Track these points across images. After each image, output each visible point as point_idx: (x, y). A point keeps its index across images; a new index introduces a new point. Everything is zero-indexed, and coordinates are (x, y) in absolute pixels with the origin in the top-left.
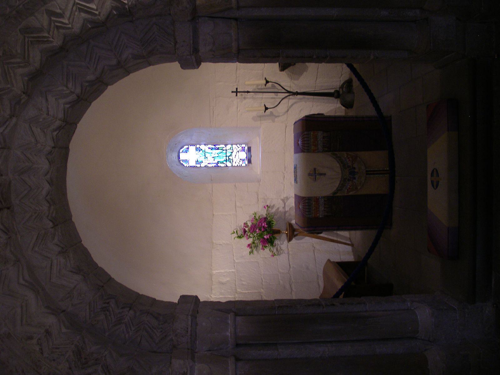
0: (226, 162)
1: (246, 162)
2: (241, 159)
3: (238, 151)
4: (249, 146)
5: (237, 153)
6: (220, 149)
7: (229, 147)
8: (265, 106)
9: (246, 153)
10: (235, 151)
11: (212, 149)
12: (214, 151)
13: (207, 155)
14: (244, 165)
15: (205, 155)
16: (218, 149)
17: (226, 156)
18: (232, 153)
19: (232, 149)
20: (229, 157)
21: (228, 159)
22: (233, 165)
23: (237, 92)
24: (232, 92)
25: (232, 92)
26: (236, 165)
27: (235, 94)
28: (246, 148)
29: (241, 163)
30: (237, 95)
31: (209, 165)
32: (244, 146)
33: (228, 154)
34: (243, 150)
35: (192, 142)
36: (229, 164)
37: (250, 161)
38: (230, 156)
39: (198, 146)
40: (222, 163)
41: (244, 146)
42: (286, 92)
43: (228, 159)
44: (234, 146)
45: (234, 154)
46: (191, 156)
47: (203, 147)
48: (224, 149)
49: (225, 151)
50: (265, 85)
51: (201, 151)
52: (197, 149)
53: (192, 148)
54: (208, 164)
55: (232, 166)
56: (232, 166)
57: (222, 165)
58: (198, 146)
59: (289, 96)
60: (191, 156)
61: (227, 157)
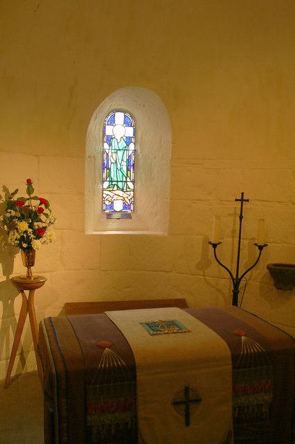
0: (109, 181)
1: (108, 211)
2: (112, 203)
3: (124, 200)
4: (133, 216)
5: (122, 198)
6: (129, 172)
7: (131, 185)
8: (220, 243)
9: (121, 211)
10: (125, 195)
11: (128, 161)
12: (125, 164)
13: (120, 153)
14: (105, 208)
15: (119, 150)
16: (128, 170)
17: (117, 181)
18: (123, 190)
19: (128, 190)
20: (117, 185)
21: (114, 183)
22: (104, 192)
23: (242, 200)
24: (243, 194)
25: (243, 194)
26: (104, 196)
27: (240, 198)
28: (129, 211)
29: (107, 203)
30: (237, 200)
31: (105, 155)
32: (132, 208)
33: (120, 184)
34: (125, 206)
35: (139, 134)
36: (106, 184)
37: (109, 216)
38: (118, 187)
39: (133, 140)
40: (109, 175)
41: (132, 208)
42: (239, 277)
43: (114, 183)
44: (132, 193)
45: (121, 193)
46: (119, 129)
47: (132, 147)
48: (128, 180)
49: (125, 180)
50: (256, 244)
51: (125, 145)
52: (130, 138)
53: (130, 132)
54: (107, 154)
55: (103, 190)
56: (103, 190)
57: (105, 176)
58: (133, 140)
59: (233, 279)
60: (119, 129)
61: (116, 183)
